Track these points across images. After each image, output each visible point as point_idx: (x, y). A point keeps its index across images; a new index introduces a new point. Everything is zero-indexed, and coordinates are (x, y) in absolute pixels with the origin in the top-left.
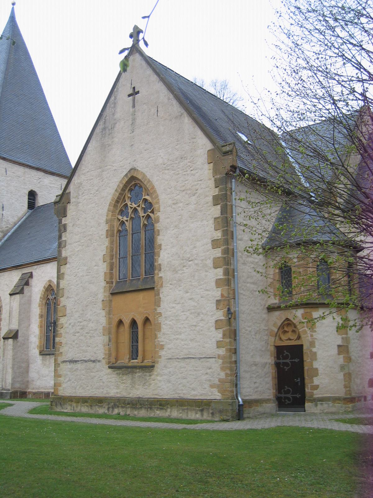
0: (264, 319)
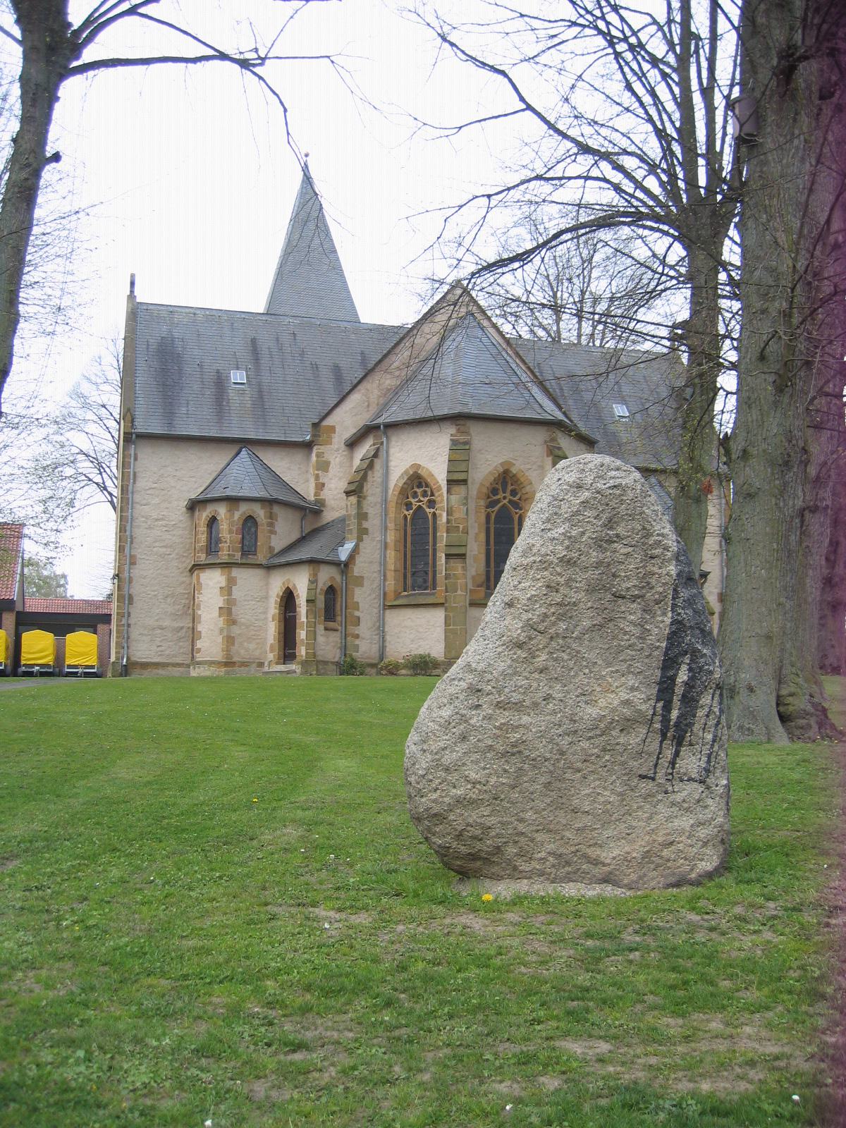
0: (183, 582)
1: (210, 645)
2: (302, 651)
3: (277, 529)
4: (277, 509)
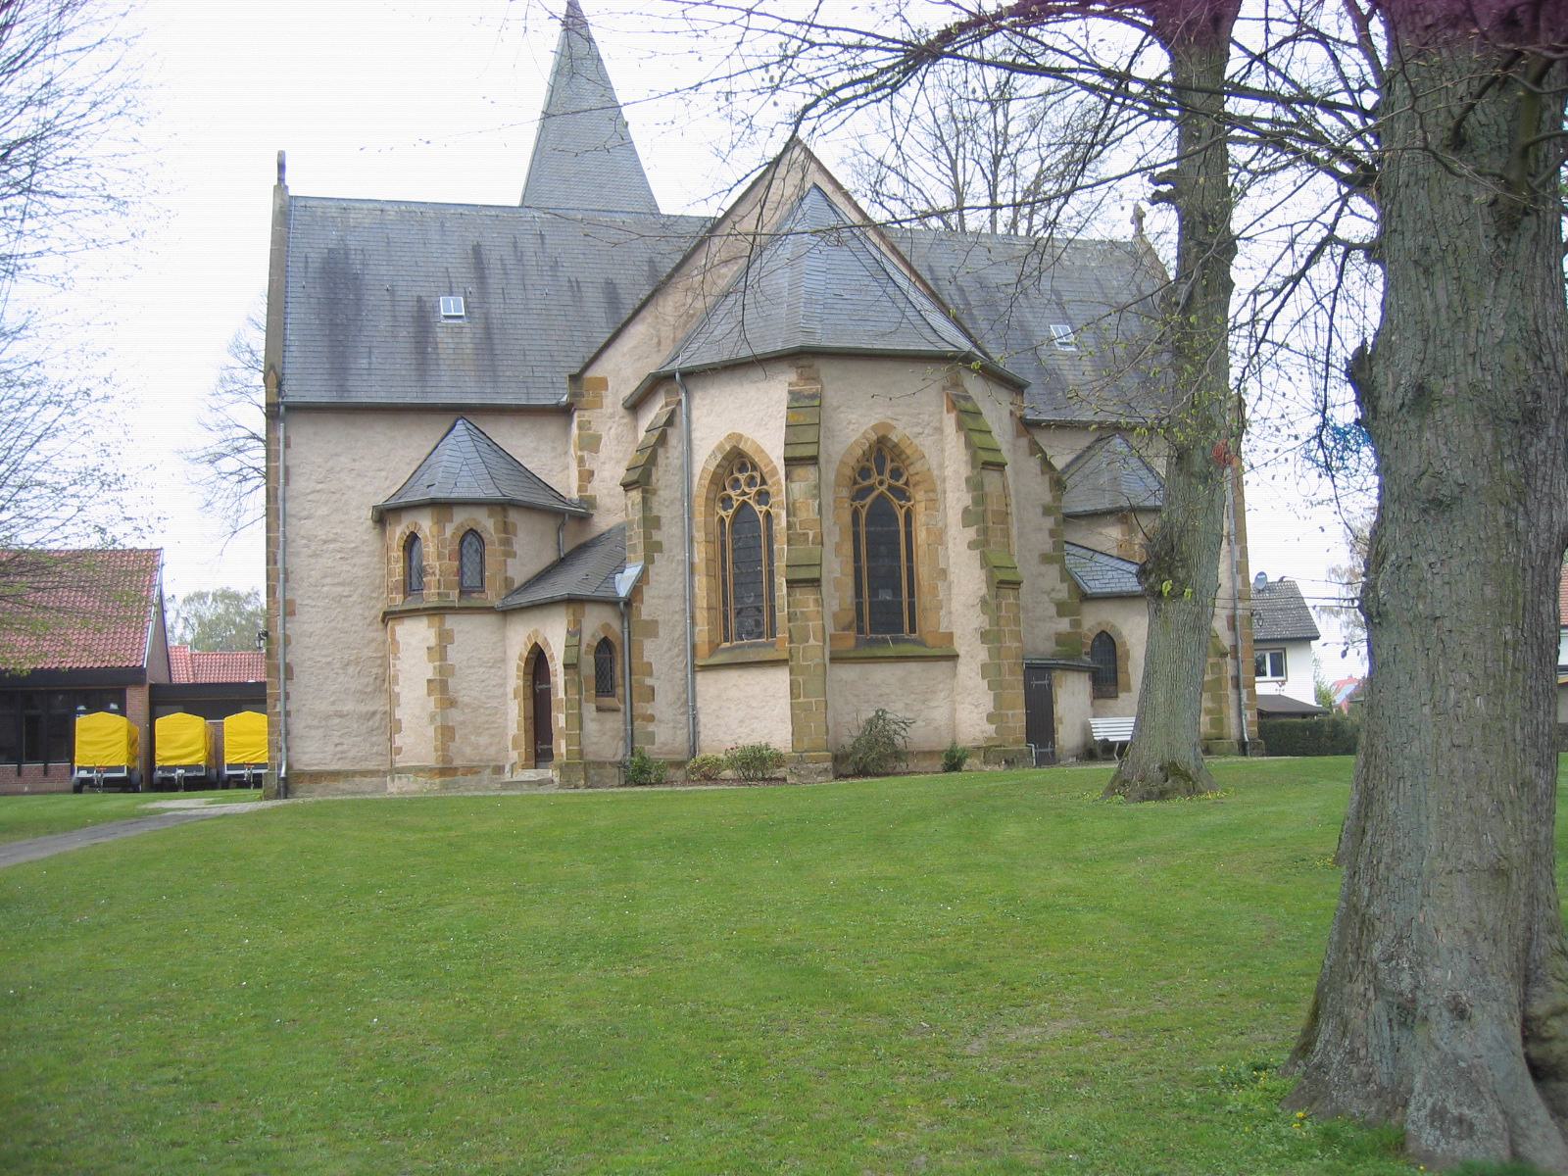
0: (373, 640)
1: (417, 742)
2: (561, 747)
3: (516, 547)
4: (514, 516)
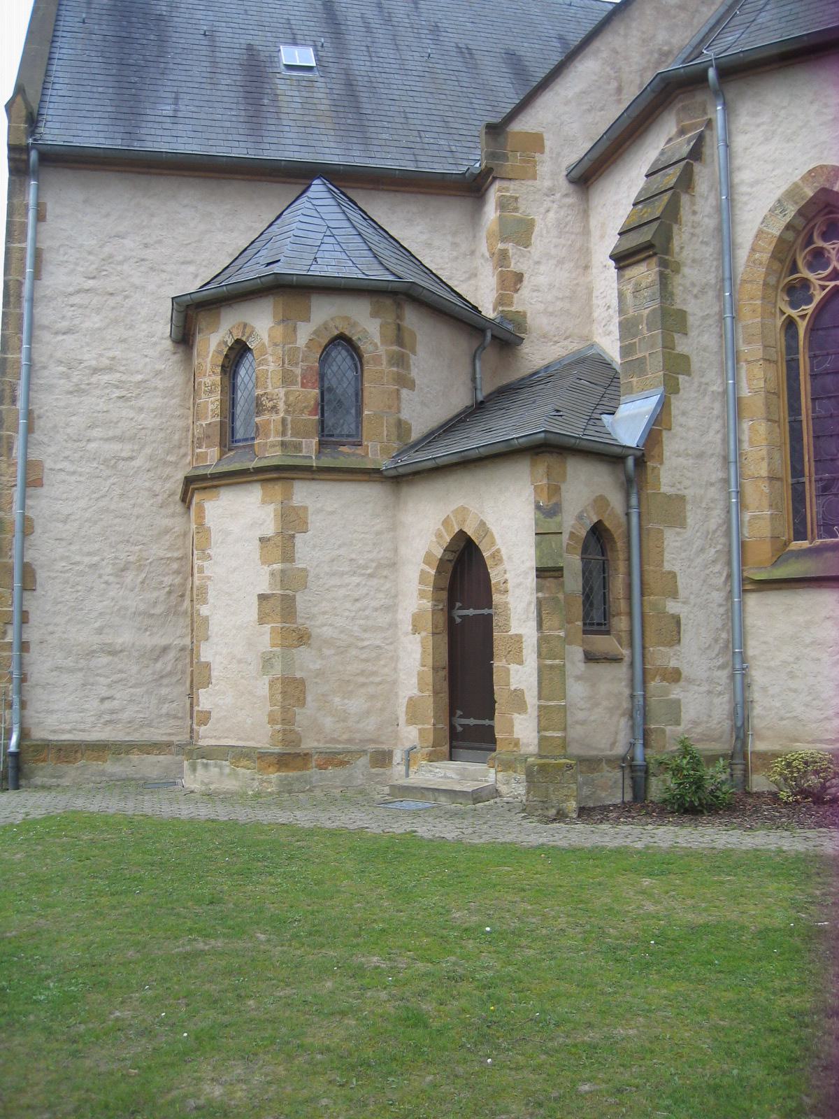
0: (167, 531)
1: (237, 704)
2: (521, 729)
3: (414, 373)
4: (412, 319)
